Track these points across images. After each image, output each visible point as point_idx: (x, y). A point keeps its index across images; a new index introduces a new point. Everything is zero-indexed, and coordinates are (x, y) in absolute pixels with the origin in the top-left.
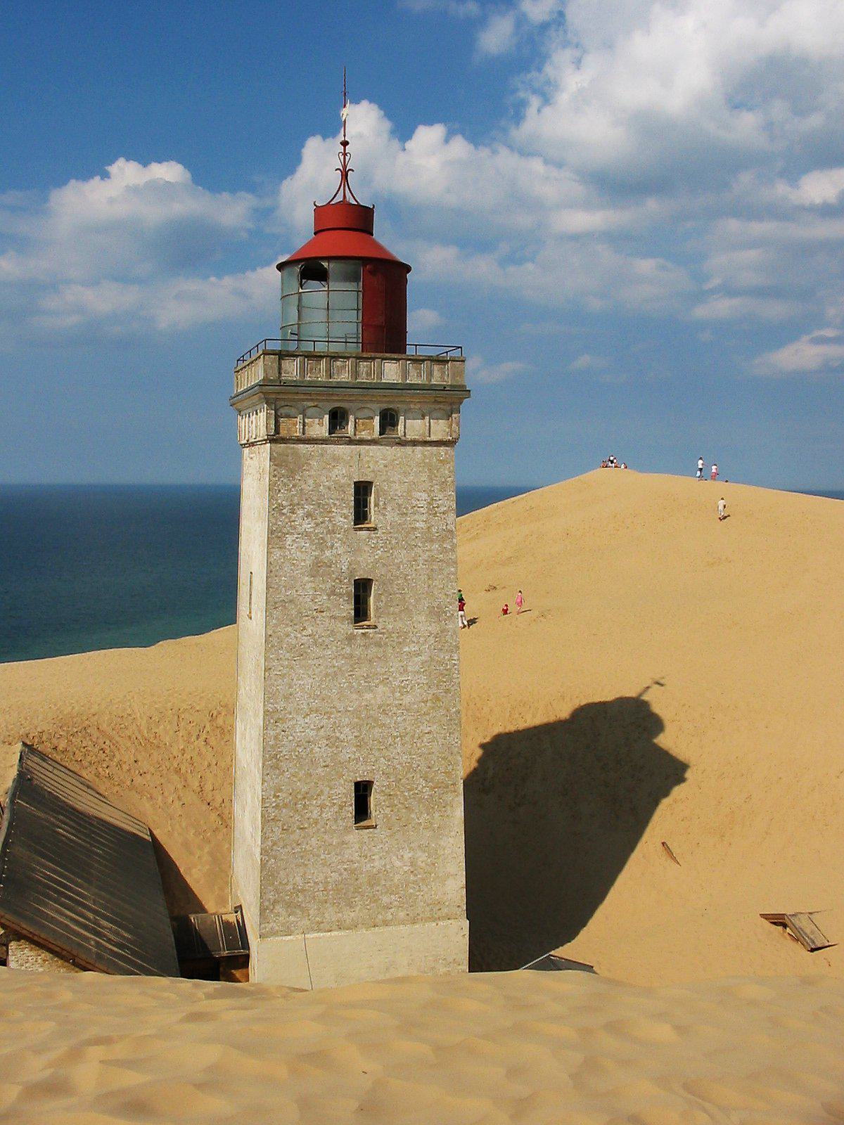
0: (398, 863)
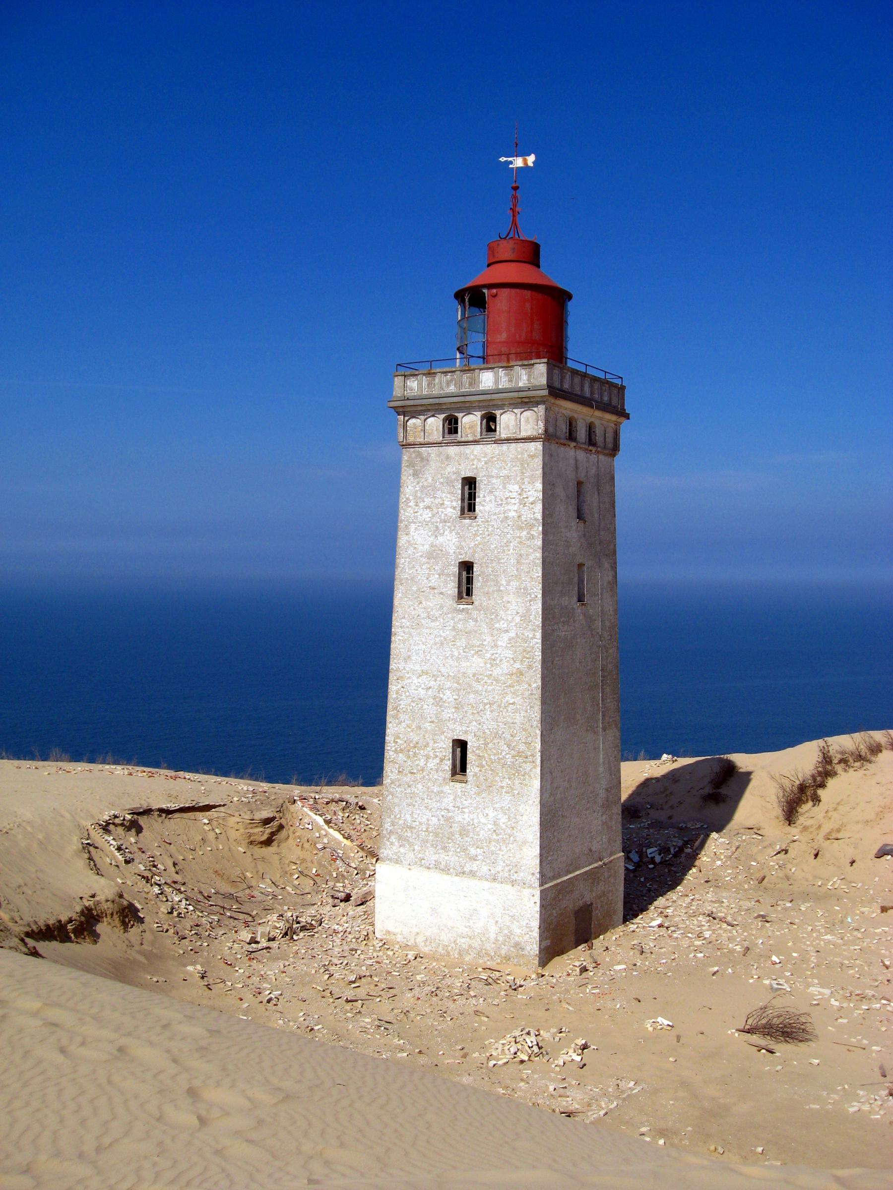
0: (483, 820)
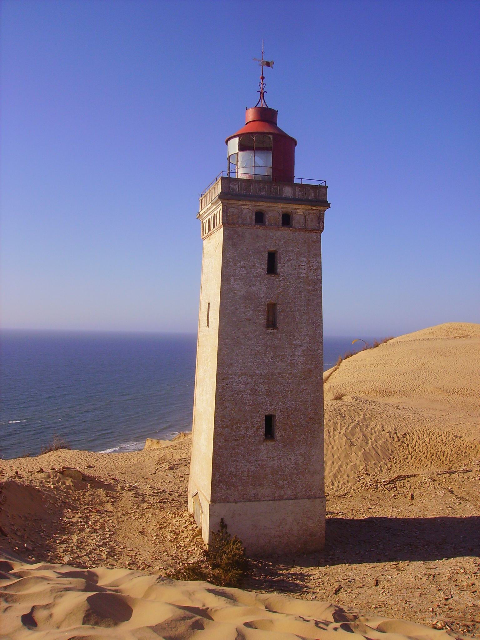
0: (288, 463)
